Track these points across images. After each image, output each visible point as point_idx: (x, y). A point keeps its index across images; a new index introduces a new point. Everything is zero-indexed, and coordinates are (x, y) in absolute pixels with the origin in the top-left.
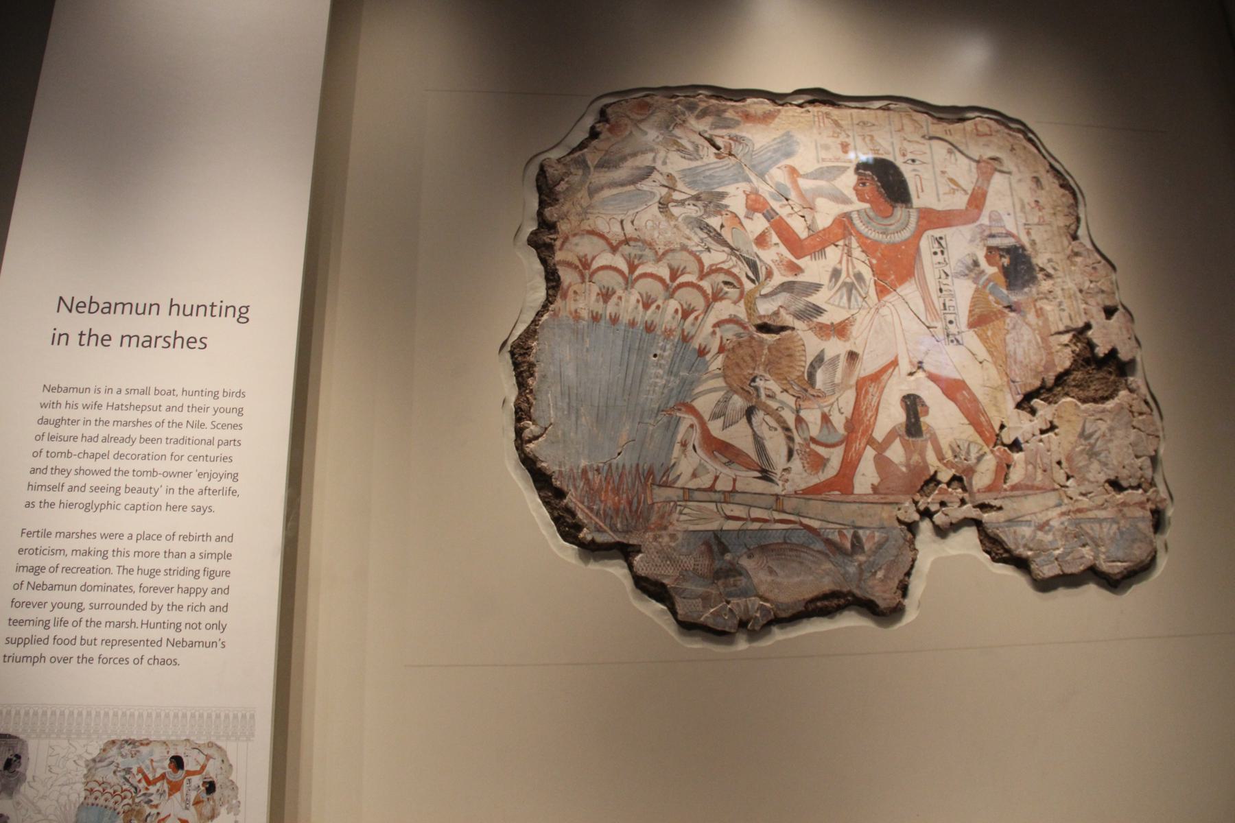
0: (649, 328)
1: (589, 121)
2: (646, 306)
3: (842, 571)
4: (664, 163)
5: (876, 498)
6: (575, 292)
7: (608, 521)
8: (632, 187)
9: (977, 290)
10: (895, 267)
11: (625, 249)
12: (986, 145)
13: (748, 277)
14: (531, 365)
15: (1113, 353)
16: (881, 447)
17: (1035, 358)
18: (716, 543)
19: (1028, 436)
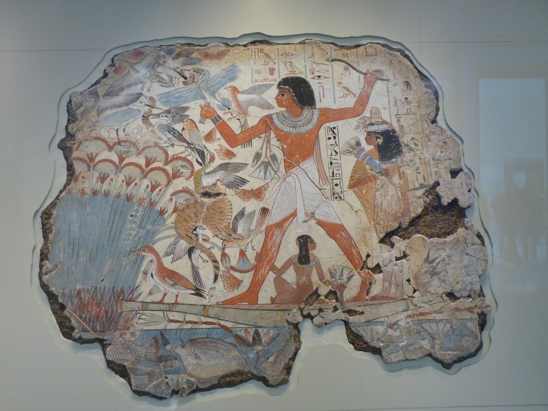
0: (129, 198)
1: (105, 65)
2: (128, 184)
3: (245, 357)
4: (149, 90)
5: (273, 307)
6: (83, 177)
7: (91, 325)
8: (126, 108)
9: (357, 162)
10: (300, 149)
11: (118, 148)
12: (372, 62)
13: (198, 162)
14: (51, 225)
15: (455, 201)
17: (396, 208)
18: (161, 338)
19: (386, 262)
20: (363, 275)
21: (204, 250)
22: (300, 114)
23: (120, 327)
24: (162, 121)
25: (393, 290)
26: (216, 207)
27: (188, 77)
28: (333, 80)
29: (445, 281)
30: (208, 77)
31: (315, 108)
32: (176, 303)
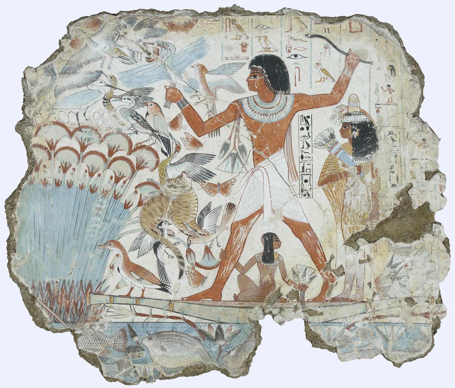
0: (93, 190)
2: (91, 175)
4: (109, 67)
6: (45, 166)
7: (62, 316)
8: (85, 88)
10: (269, 140)
11: (78, 134)
13: (163, 151)
16: (243, 270)
18: (130, 331)
20: (325, 276)
22: (273, 100)
23: (89, 319)
24: (125, 104)
25: (353, 292)
26: (182, 201)
27: (152, 52)
28: (311, 60)
29: (405, 286)
30: (173, 53)
31: (289, 94)
32: (142, 297)
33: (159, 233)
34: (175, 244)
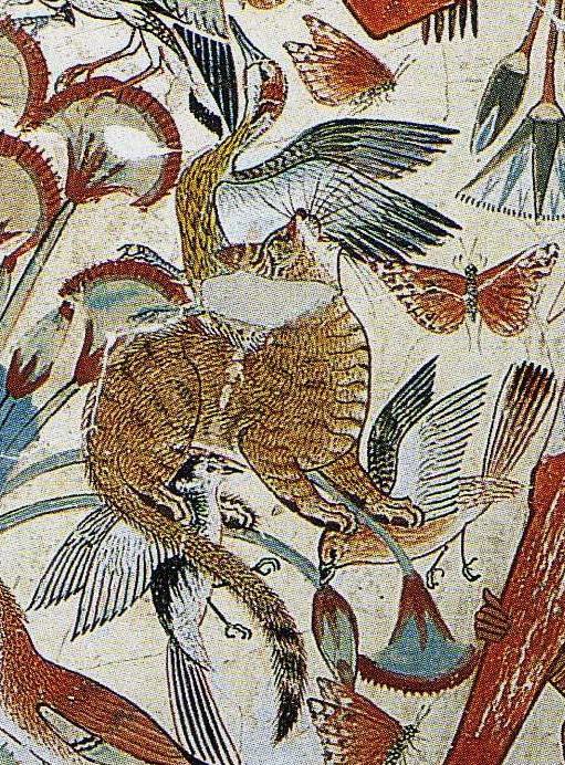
13: (197, 108)
21: (228, 572)
33: (178, 514)
34: (257, 568)
